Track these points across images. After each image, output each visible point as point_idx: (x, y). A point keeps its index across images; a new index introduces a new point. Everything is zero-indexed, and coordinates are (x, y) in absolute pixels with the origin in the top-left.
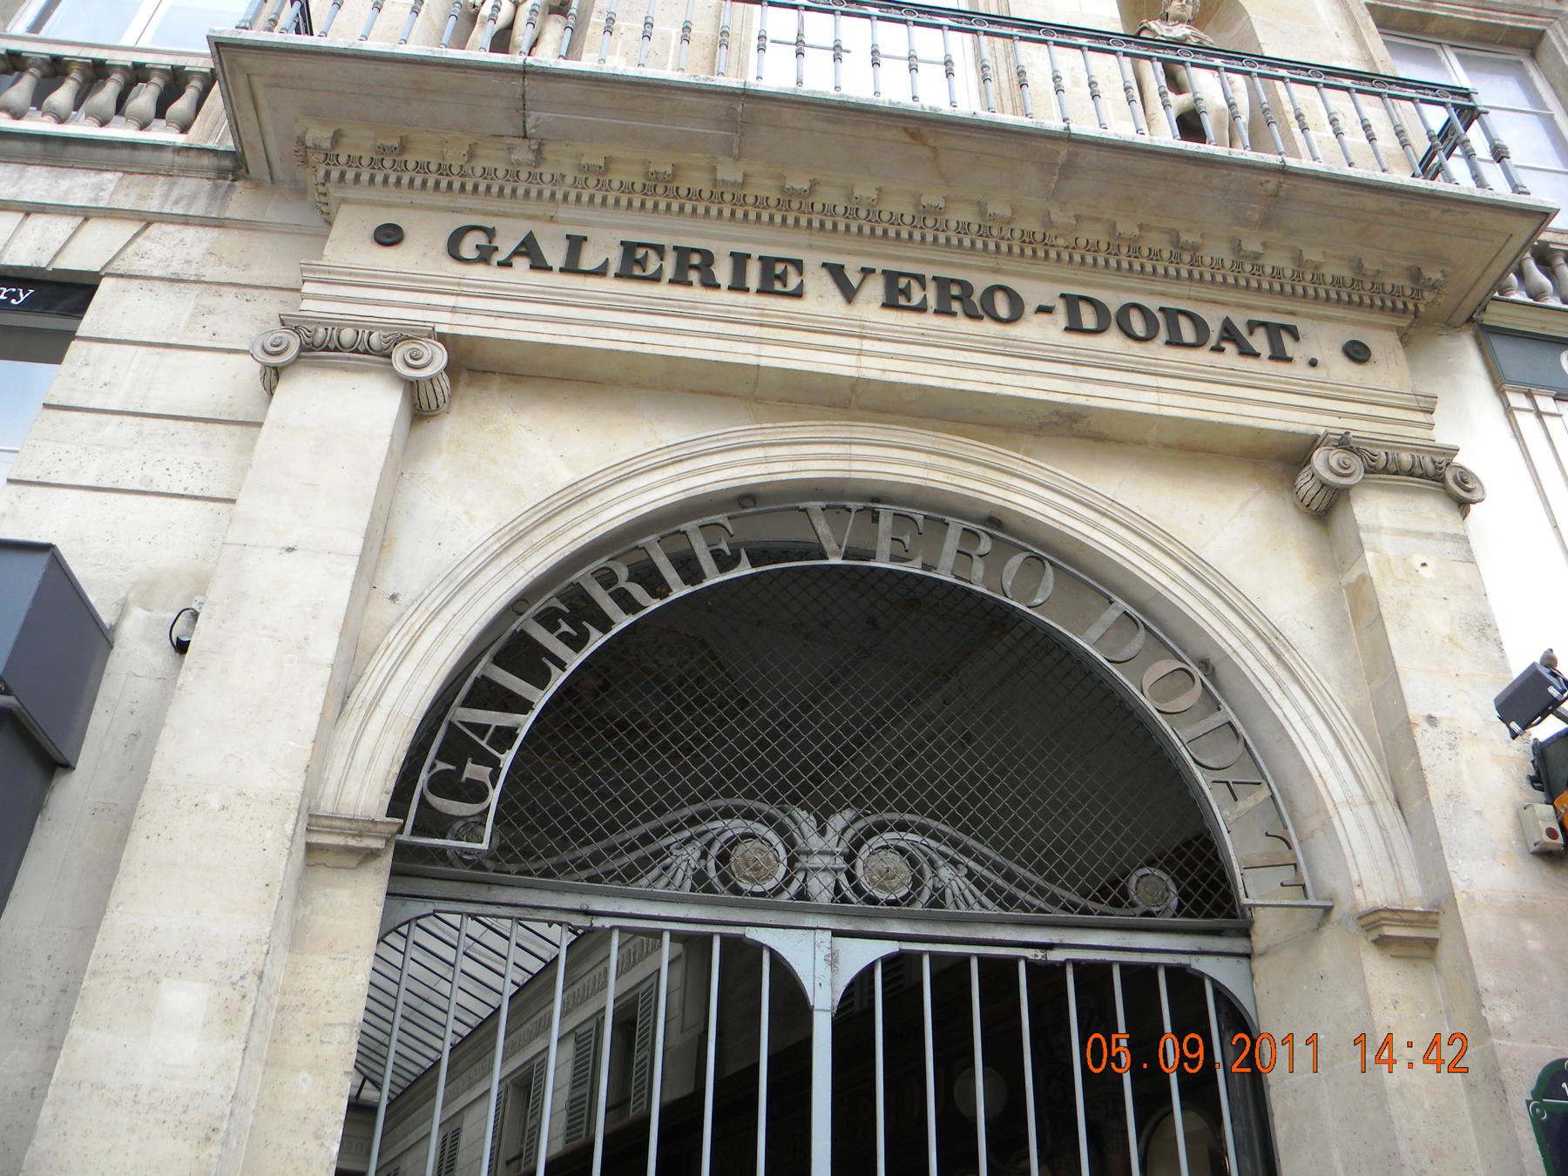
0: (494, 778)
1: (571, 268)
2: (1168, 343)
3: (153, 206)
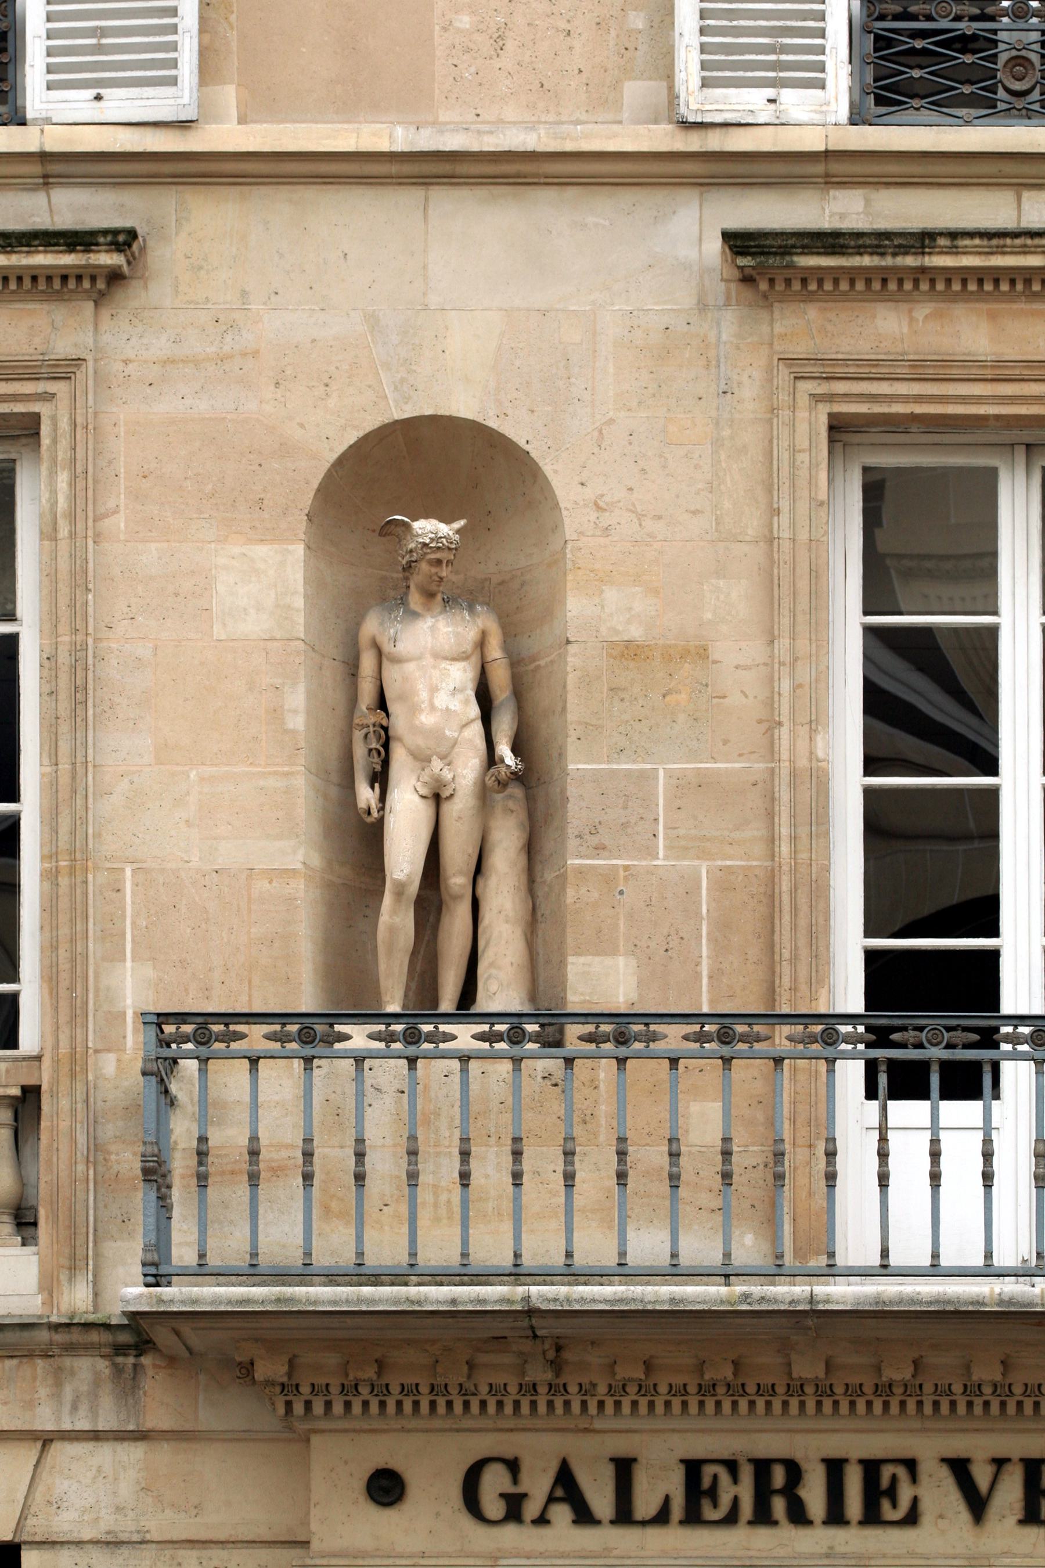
1: (624, 1516)
3: (45, 1420)
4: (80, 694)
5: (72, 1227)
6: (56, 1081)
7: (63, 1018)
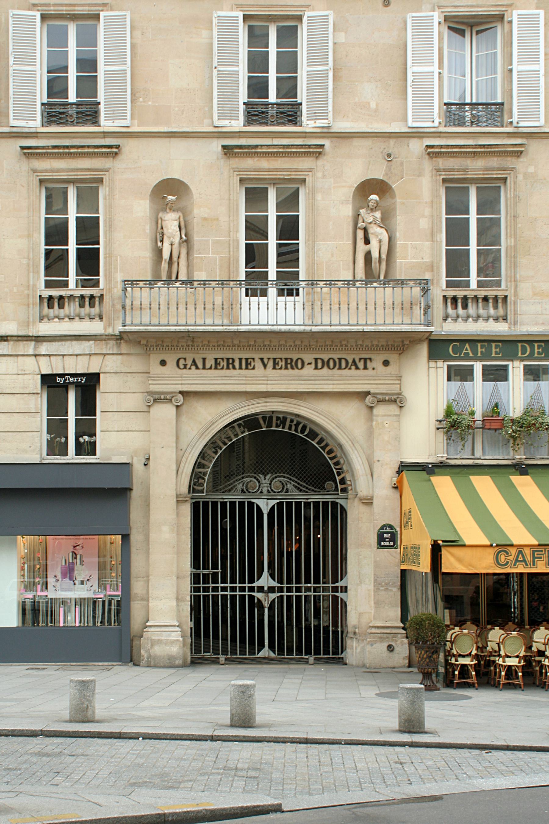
0: (205, 481)
2: (338, 369)
4: (110, 226)
5: (109, 318)
6: (106, 293)
7: (108, 282)
